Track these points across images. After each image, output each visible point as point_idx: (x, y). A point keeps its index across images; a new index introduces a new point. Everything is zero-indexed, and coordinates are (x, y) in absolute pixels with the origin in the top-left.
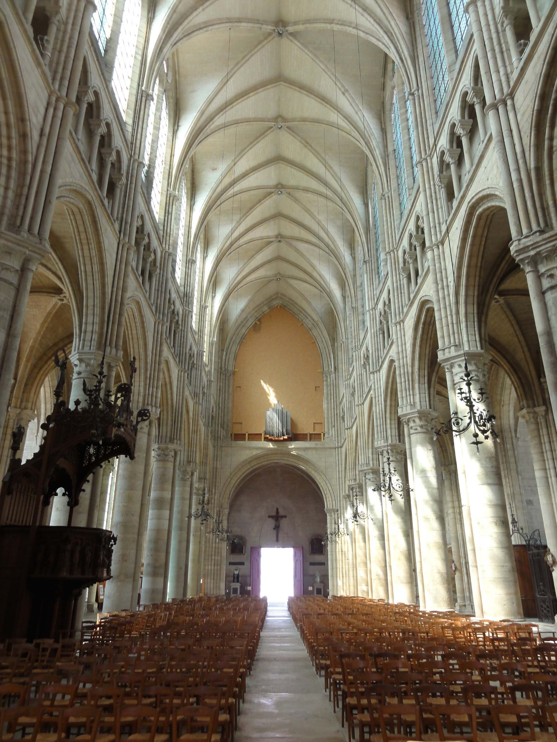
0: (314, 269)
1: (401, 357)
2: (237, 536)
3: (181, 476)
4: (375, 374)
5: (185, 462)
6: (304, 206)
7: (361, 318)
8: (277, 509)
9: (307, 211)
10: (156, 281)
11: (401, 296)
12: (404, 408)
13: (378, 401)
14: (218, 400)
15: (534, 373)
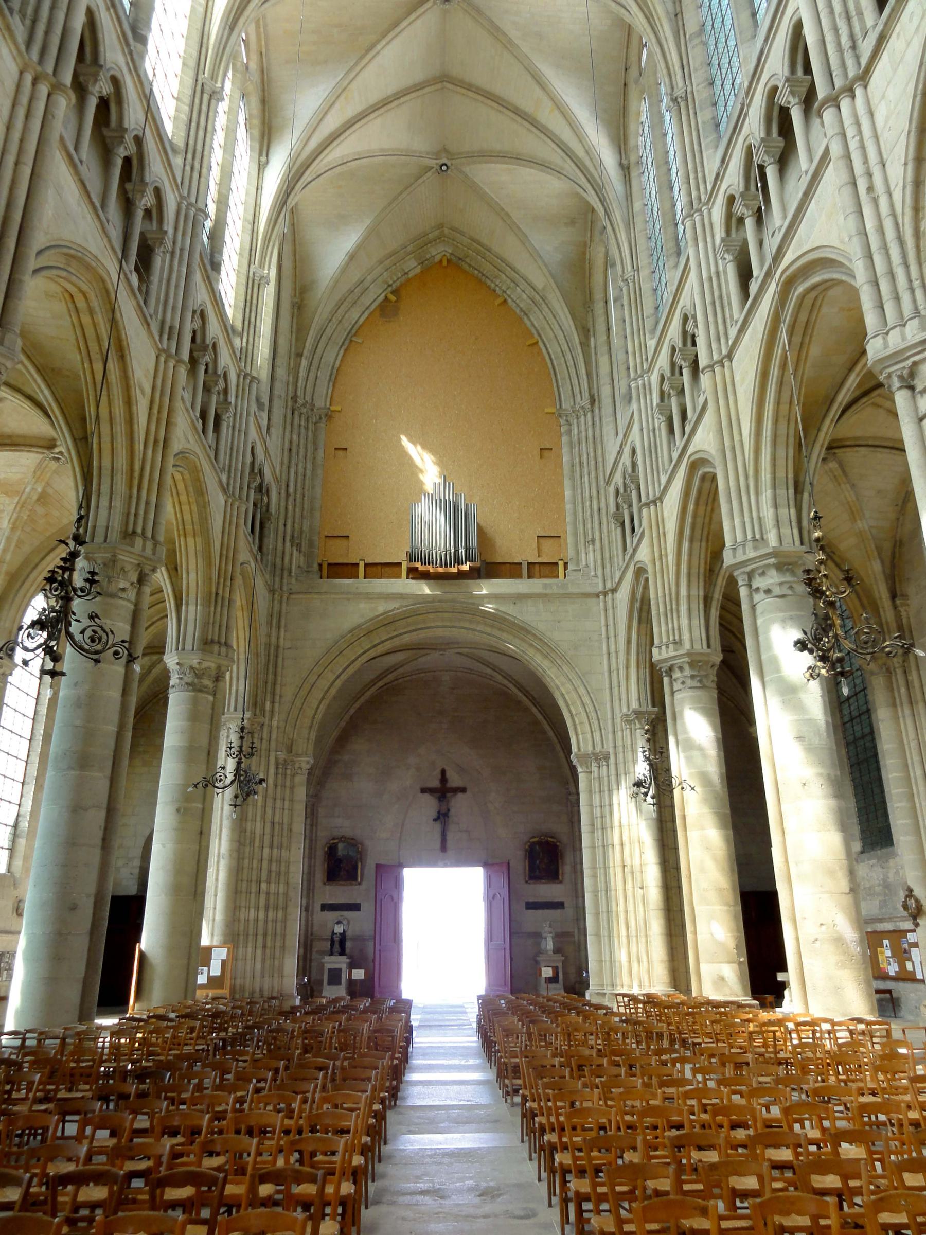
2: (342, 839)
5: (114, 536)
7: (704, 116)
8: (443, 772)
13: (870, 189)
14: (284, 477)
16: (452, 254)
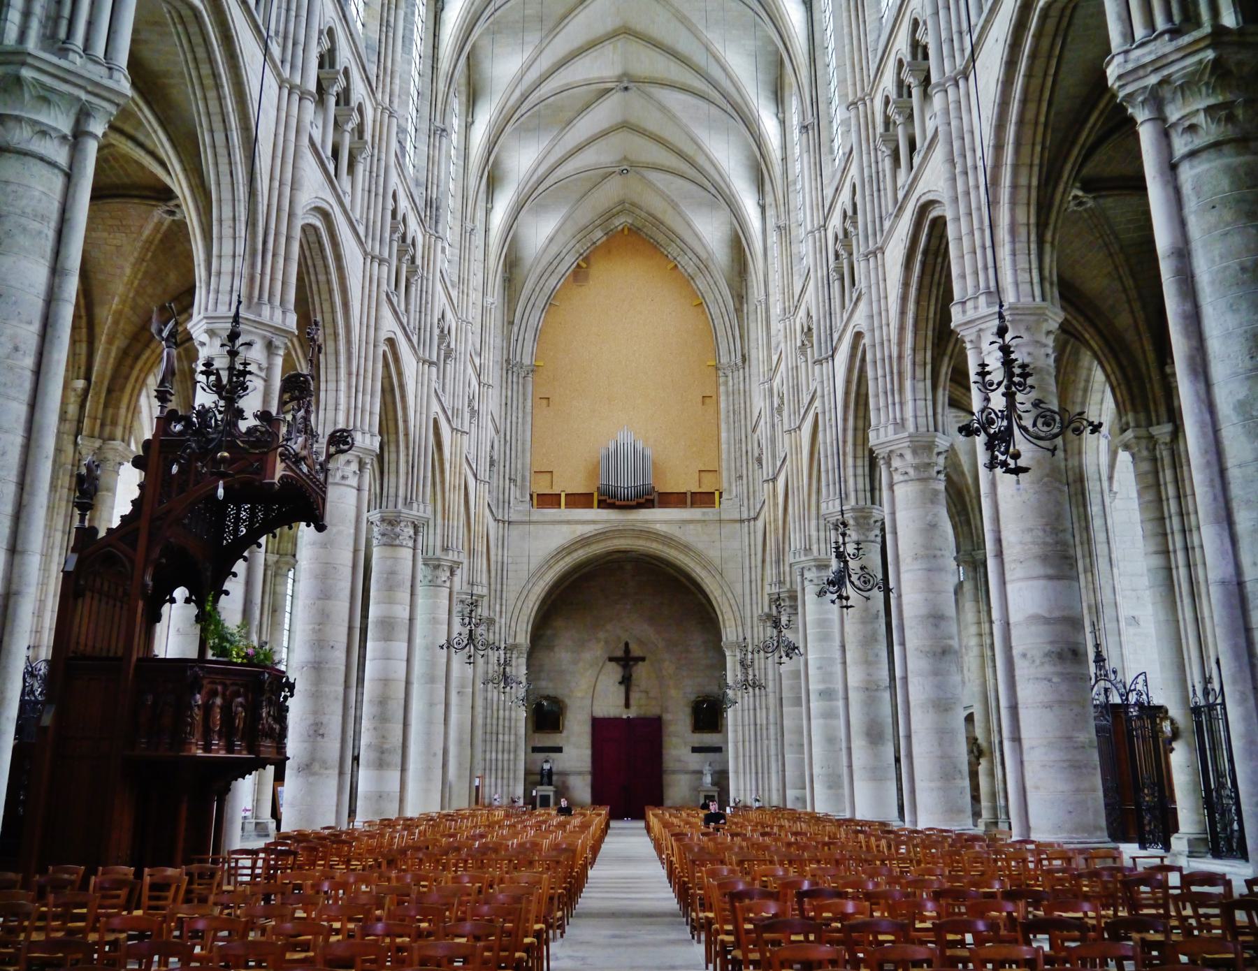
0: (700, 147)
1: (876, 324)
2: (547, 698)
3: (430, 578)
4: (825, 365)
6: (677, 11)
8: (627, 644)
9: (684, 20)
10: (365, 170)
11: (879, 197)
12: (882, 431)
13: (830, 420)
15: (1151, 356)
16: (632, 224)
